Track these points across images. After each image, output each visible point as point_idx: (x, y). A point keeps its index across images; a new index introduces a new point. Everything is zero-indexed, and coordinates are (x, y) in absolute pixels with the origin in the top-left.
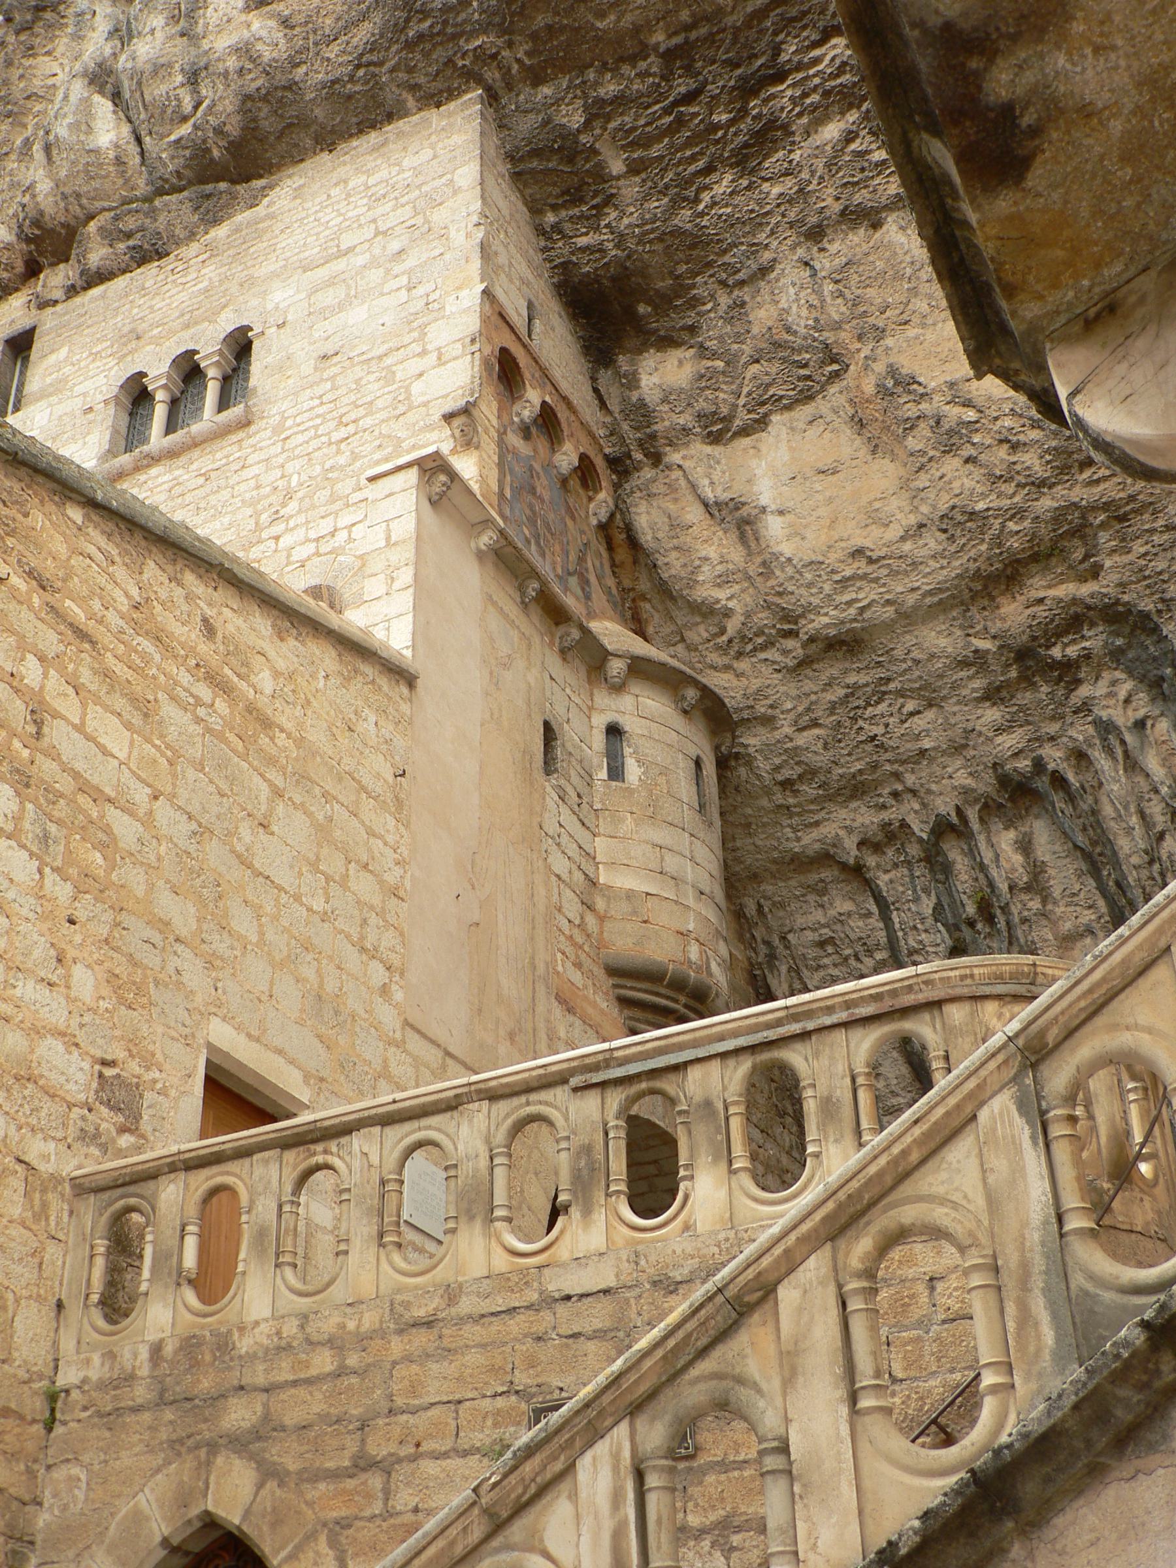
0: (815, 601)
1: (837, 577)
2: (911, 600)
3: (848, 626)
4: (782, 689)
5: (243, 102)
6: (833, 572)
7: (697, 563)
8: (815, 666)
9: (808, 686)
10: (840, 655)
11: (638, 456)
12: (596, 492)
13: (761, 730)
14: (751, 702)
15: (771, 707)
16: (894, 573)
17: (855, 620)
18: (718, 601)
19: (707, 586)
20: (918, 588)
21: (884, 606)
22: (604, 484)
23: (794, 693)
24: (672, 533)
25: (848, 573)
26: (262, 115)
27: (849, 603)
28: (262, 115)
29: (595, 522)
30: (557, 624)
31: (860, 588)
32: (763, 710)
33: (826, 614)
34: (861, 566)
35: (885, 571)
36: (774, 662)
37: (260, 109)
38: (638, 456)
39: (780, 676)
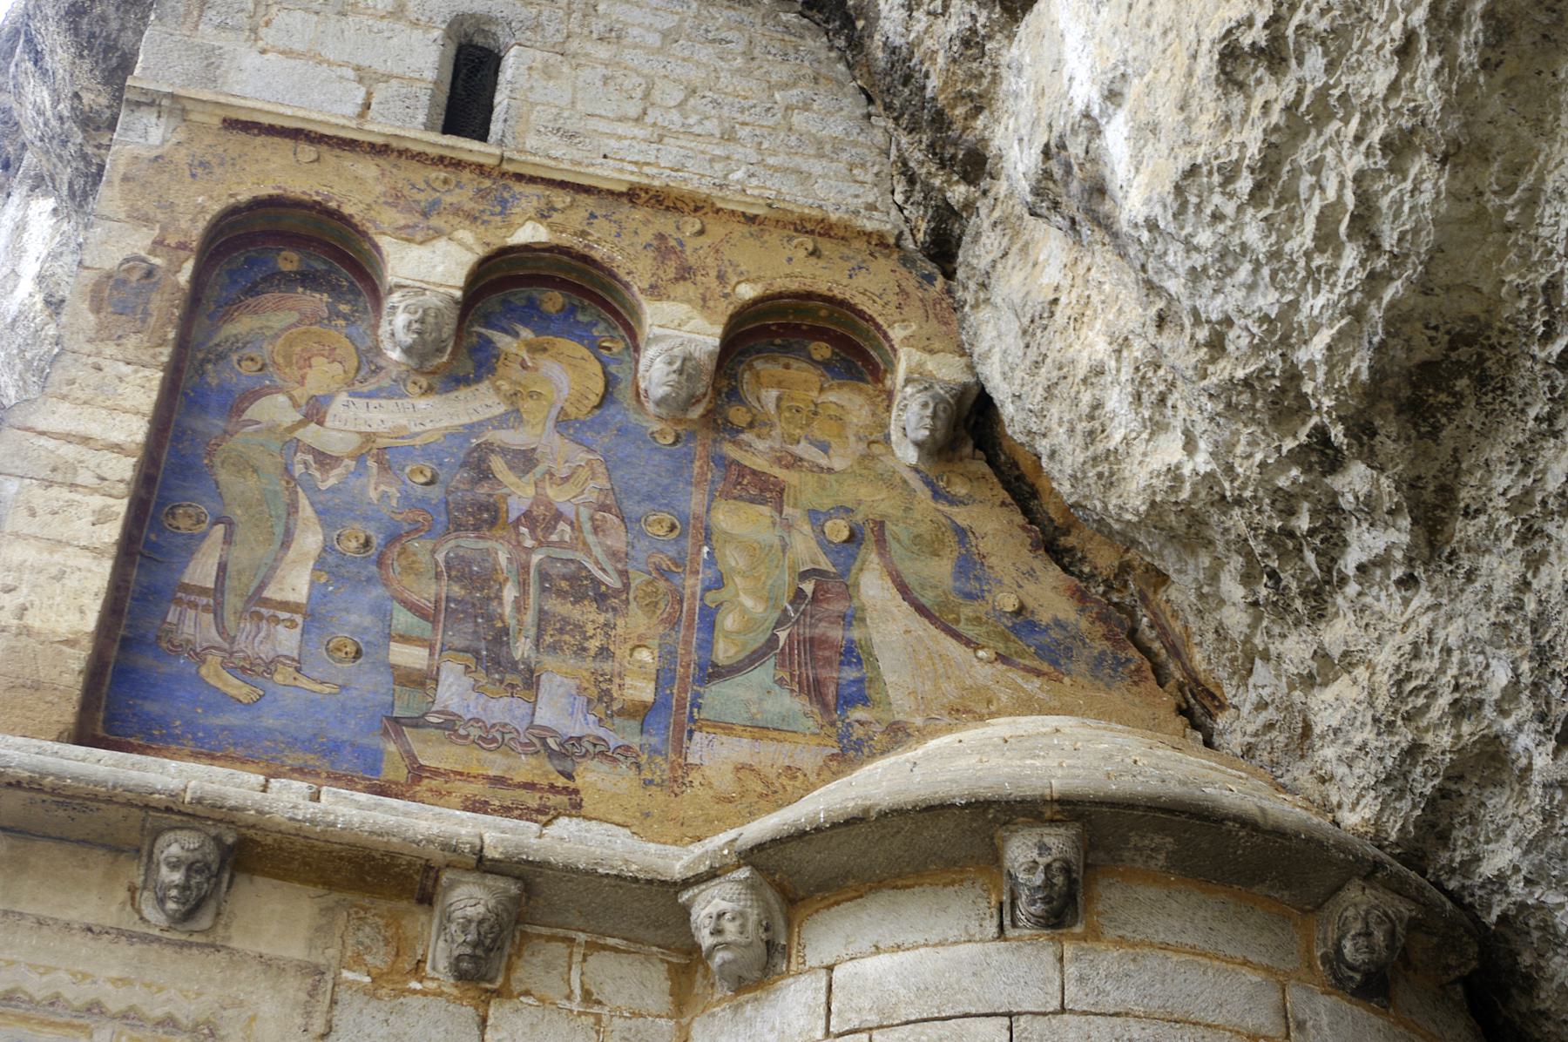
0: (1268, 300)
1: (1245, 184)
2: (1427, 90)
3: (1376, 313)
4: (1452, 633)
5: (75, 30)
6: (1229, 175)
7: (1086, 398)
8: (1465, 495)
9: (1501, 569)
10: (1470, 414)
11: (958, 193)
12: (891, 367)
13: (1500, 804)
14: (1405, 737)
15: (1460, 710)
16: (1337, 44)
17: (1375, 282)
18: (1174, 474)
19: (1138, 448)
20: (1410, 37)
21: (1397, 169)
22: (897, 334)
23: (1482, 624)
24: (1033, 354)
25: (1252, 140)
26: (114, 25)
27: (1325, 239)
28: (114, 25)
29: (911, 455)
30: (426, 899)
31: (1317, 167)
32: (1446, 740)
33: (1316, 328)
34: (1274, 92)
35: (1315, 60)
36: (1383, 561)
37: (103, 19)
38: (958, 193)
39: (1423, 597)
